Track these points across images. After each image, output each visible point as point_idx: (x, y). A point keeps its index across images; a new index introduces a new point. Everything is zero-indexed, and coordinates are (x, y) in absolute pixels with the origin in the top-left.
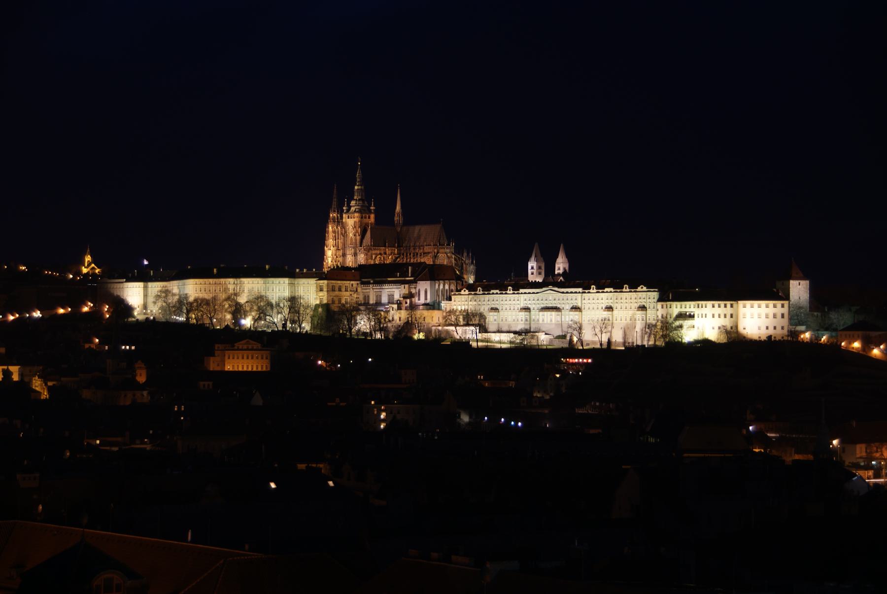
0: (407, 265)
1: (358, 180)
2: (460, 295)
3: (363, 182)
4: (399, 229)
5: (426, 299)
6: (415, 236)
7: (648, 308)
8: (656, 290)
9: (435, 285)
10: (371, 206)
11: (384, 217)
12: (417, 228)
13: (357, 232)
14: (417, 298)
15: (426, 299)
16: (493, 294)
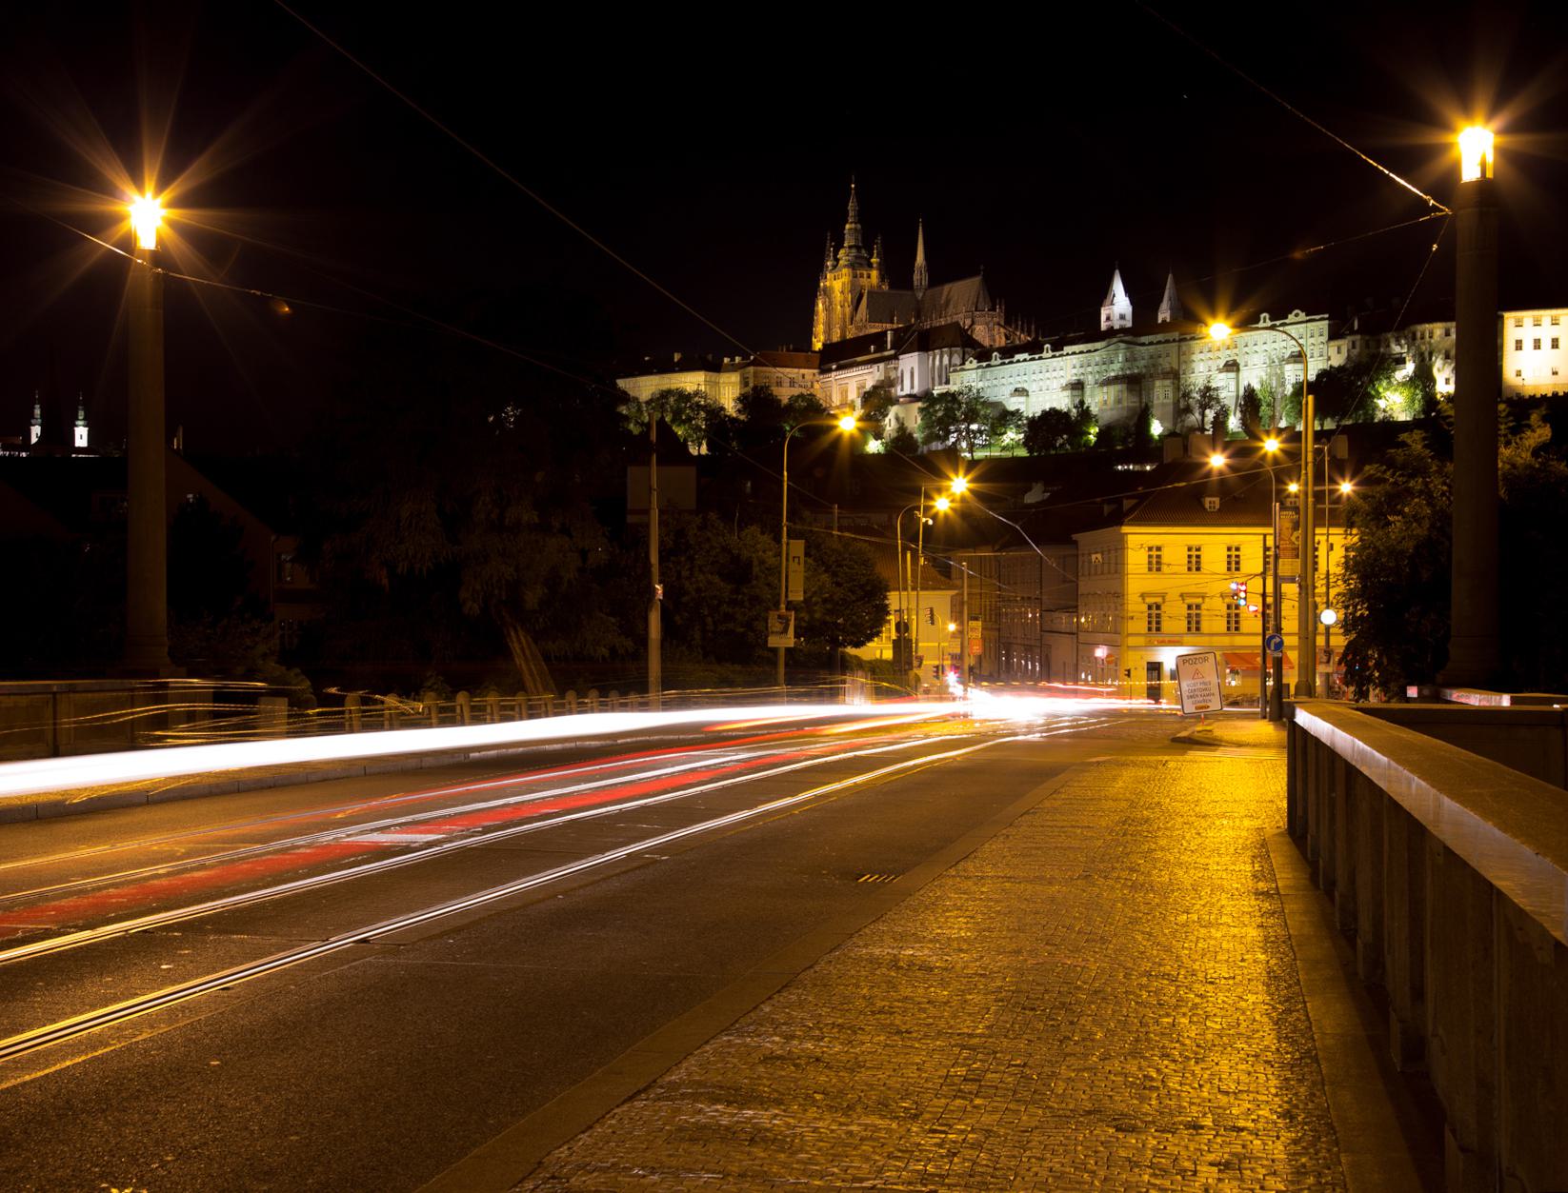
0: (884, 334)
1: (851, 213)
2: (964, 370)
3: (861, 218)
4: (921, 295)
5: (912, 387)
6: (942, 302)
7: (1308, 356)
8: (1326, 316)
9: (928, 359)
10: (871, 256)
11: (897, 272)
12: (947, 287)
13: (845, 300)
14: (899, 388)
15: (912, 387)
16: (1018, 361)
